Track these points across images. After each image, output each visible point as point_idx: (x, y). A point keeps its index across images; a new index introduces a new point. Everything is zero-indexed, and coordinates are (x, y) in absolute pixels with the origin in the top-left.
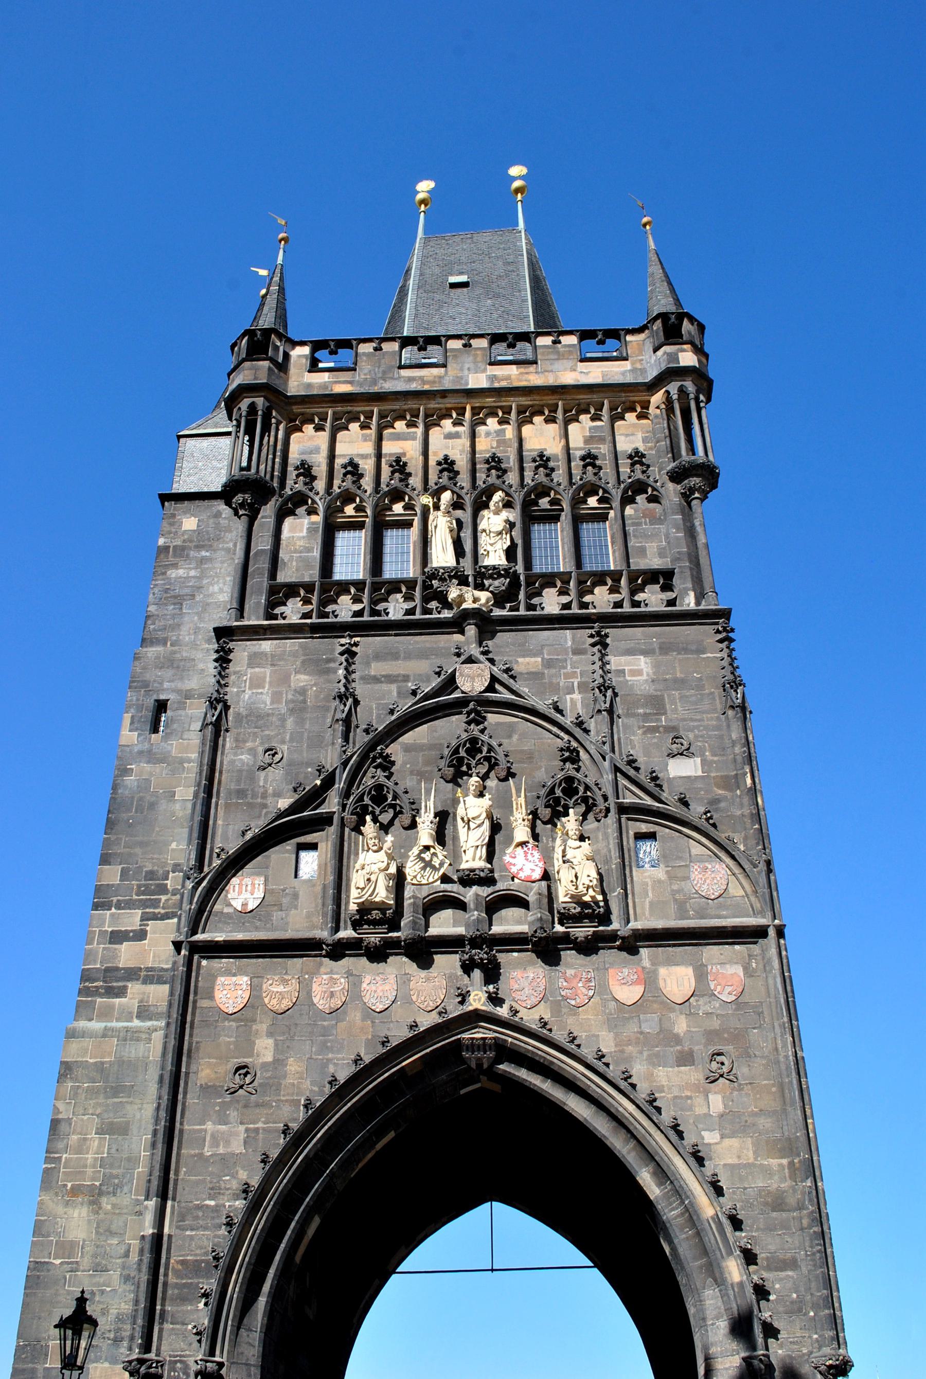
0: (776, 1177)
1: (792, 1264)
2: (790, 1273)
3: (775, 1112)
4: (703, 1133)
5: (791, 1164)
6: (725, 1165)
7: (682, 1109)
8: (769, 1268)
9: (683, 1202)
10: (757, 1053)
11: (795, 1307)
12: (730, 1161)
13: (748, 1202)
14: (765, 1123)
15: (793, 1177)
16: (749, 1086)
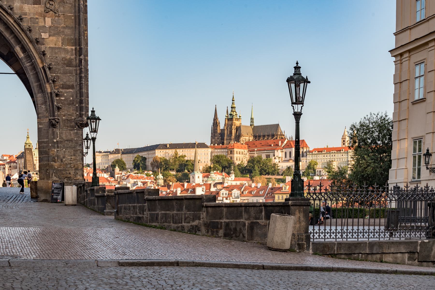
0: (69, 54)
1: (72, 87)
2: (71, 90)
3: (72, 27)
4: (42, 34)
5: (76, 49)
6: (49, 47)
7: (34, 23)
8: (63, 88)
9: (31, 61)
10: (68, 2)
11: (71, 103)
12: (52, 46)
13: (57, 62)
14: (68, 31)
15: (76, 54)
16: (63, 16)
